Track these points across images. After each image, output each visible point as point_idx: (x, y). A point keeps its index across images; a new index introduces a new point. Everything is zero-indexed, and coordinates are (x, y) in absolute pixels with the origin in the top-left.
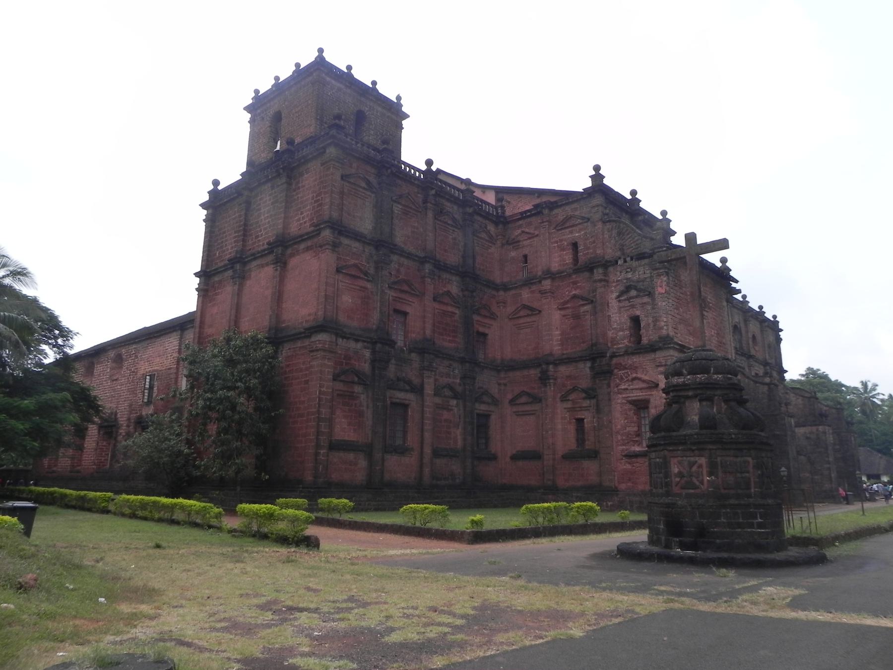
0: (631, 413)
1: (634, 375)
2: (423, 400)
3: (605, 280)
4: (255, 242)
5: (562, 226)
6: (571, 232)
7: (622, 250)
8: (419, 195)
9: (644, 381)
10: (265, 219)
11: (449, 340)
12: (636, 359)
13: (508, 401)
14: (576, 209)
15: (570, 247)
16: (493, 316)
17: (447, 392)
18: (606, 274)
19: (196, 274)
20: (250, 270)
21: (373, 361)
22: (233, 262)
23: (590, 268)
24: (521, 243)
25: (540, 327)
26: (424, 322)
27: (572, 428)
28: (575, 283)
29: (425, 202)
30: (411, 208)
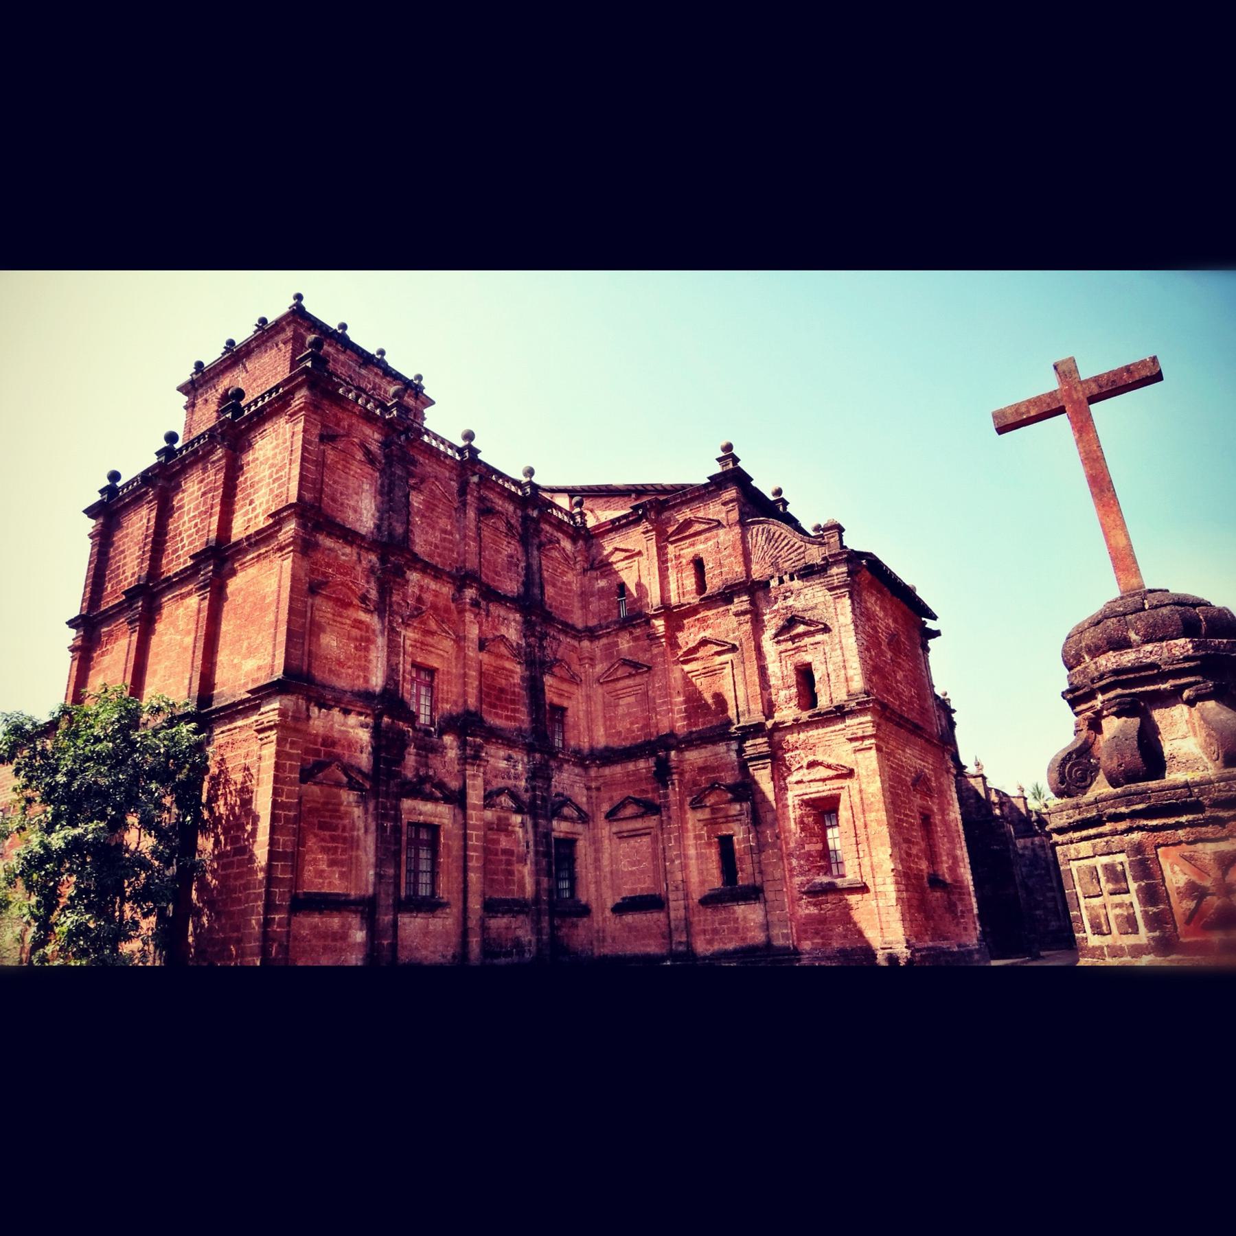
1: (811, 758)
2: (465, 817)
4: (172, 560)
6: (693, 545)
7: (774, 564)
8: (452, 483)
9: (829, 767)
10: (190, 521)
11: (506, 716)
12: (814, 734)
15: (692, 565)
16: (574, 680)
17: (505, 800)
19: (72, 623)
21: (376, 751)
22: (131, 594)
24: (615, 566)
25: (650, 692)
26: (465, 684)
27: (713, 853)
28: (704, 620)
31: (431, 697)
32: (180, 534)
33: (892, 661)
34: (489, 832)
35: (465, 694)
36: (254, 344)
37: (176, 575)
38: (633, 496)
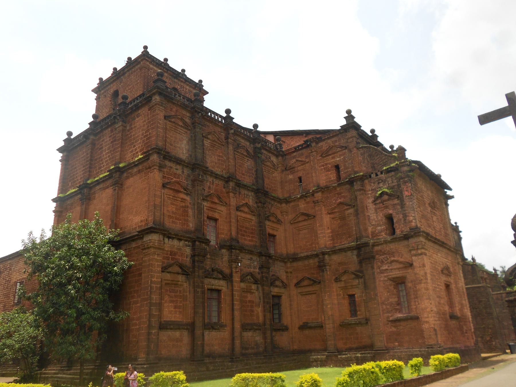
0: (392, 288)
1: (393, 259)
2: (232, 286)
3: (363, 190)
5: (325, 154)
6: (333, 158)
7: (373, 167)
8: (222, 134)
9: (401, 263)
10: (106, 155)
11: (249, 240)
12: (392, 246)
13: (294, 284)
14: (336, 141)
15: (334, 168)
16: (279, 222)
18: (363, 185)
20: (94, 193)
23: (351, 182)
24: (296, 169)
25: (315, 228)
26: (230, 226)
28: (339, 194)
29: (227, 138)
30: (217, 142)
31: (216, 232)
32: (102, 160)
33: (431, 212)
34: (243, 293)
35: (230, 230)
36: (126, 70)
38: (304, 135)
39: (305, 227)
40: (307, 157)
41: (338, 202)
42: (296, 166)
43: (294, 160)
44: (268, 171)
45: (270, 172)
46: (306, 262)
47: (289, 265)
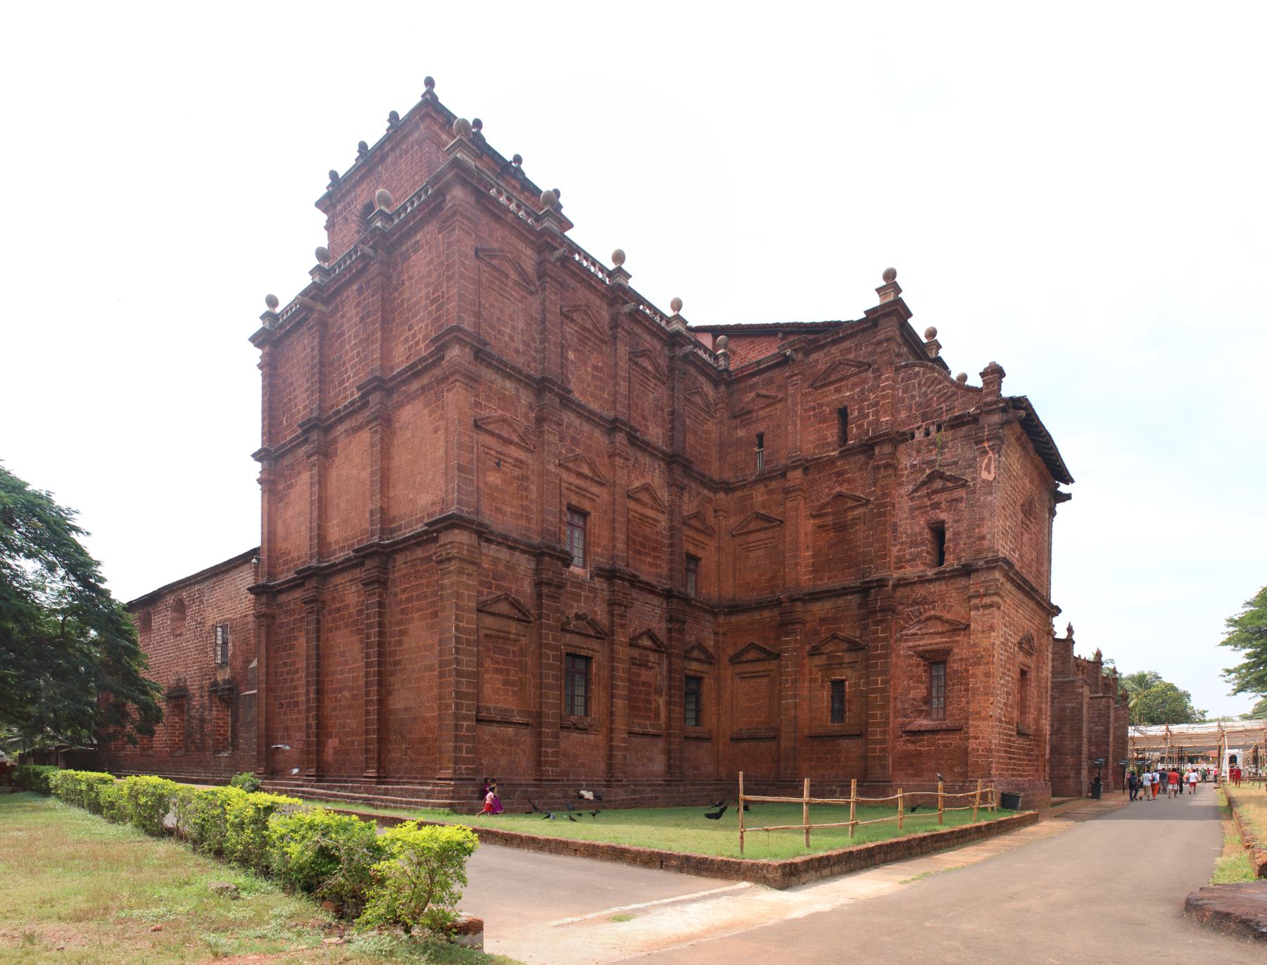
4: (340, 392)
5: (821, 381)
6: (838, 391)
15: (836, 415)
20: (335, 441)
23: (867, 448)
31: (584, 540)
33: (1022, 522)
34: (633, 667)
37: (346, 407)
39: (759, 543)
40: (779, 388)
41: (834, 492)
42: (755, 408)
43: (753, 395)
44: (695, 416)
45: (698, 418)
46: (757, 616)
47: (721, 619)
